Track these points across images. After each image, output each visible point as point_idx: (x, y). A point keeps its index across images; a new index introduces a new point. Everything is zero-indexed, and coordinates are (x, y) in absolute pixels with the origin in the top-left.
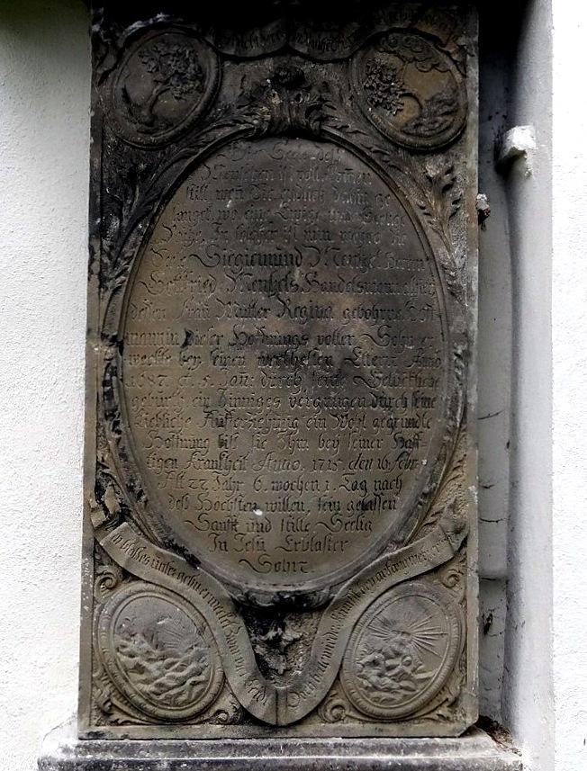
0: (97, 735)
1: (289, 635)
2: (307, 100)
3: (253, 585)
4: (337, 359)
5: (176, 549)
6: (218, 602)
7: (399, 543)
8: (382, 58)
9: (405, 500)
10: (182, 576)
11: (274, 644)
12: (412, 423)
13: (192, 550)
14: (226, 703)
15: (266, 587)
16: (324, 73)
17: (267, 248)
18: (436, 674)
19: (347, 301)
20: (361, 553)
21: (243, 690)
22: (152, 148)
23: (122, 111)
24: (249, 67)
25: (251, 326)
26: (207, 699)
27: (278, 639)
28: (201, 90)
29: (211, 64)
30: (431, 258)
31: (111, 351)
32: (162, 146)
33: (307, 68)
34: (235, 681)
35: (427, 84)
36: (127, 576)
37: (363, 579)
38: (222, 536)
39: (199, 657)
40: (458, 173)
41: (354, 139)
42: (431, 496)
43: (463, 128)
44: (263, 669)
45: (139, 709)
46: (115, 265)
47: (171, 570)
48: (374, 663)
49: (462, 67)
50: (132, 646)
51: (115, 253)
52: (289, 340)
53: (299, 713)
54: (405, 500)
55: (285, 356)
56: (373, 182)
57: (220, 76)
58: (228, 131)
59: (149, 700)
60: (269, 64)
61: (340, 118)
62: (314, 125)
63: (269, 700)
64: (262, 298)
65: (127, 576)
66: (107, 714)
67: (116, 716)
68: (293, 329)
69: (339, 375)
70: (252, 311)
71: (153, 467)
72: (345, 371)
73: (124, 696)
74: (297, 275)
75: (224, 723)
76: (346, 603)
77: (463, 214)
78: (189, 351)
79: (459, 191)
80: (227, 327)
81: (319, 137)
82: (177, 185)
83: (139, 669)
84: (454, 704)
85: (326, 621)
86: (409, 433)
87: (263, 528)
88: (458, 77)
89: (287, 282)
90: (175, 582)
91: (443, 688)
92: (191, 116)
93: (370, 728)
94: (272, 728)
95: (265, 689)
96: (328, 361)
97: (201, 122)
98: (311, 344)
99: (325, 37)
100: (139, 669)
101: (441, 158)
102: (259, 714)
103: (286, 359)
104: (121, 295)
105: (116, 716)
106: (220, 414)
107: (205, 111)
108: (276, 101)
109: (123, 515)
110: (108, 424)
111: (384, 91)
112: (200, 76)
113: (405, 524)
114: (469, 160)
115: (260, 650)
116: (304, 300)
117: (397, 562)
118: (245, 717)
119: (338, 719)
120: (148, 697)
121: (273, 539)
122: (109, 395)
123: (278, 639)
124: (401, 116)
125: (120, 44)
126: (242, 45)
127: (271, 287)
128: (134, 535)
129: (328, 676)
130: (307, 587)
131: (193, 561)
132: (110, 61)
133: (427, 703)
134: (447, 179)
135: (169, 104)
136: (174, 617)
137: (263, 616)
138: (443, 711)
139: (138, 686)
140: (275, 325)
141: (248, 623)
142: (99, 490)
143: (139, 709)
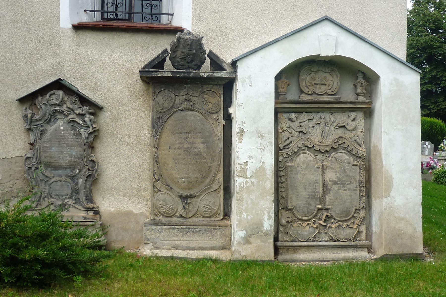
0: (155, 219)
1: (189, 202)
2: (191, 104)
3: (182, 192)
4: (197, 151)
5: (168, 186)
6: (176, 195)
7: (209, 185)
8: (205, 96)
9: (210, 177)
10: (169, 191)
11: (186, 203)
12: (211, 163)
13: (171, 186)
14: (178, 214)
15: (185, 193)
16: (195, 98)
17: (184, 131)
18: (216, 209)
19: (199, 141)
20: (202, 187)
21: (180, 211)
22: (163, 112)
23: (157, 106)
24: (181, 97)
25: (182, 145)
26: (174, 213)
27: (187, 202)
28: (172, 102)
29: (174, 97)
30: (214, 133)
31: (156, 150)
32: (165, 112)
33: (191, 97)
34: (179, 210)
35: (213, 100)
36: (159, 190)
37: (202, 192)
38: (177, 183)
39: (172, 205)
40: (219, 117)
41: (200, 111)
42: (214, 177)
43: (220, 109)
44: (184, 208)
45: (162, 215)
46: (156, 134)
47: (167, 189)
48: (204, 207)
49: (220, 97)
50: (161, 203)
51: (156, 132)
52: (188, 148)
53: (191, 216)
54: (210, 177)
55: (187, 151)
56: (203, 119)
57: (175, 99)
58: (177, 109)
59: (164, 213)
60: (184, 97)
61: (197, 106)
62: (193, 108)
63: (185, 213)
64: (183, 140)
65: (159, 190)
66: (156, 215)
67: (158, 216)
68: (189, 146)
69: (198, 154)
70: (182, 142)
71: (164, 171)
72: (198, 154)
73: (160, 212)
74: (190, 136)
75: (177, 217)
76: (199, 196)
77: (220, 125)
78: (170, 150)
79: (219, 121)
80: (177, 145)
81: (193, 111)
82: (167, 119)
83: (162, 207)
84: (219, 215)
85: (195, 199)
86: (210, 165)
87: (184, 182)
88: (219, 99)
89: (188, 137)
90: (168, 192)
91: (217, 211)
92: (170, 107)
93: (204, 219)
94: (186, 218)
95: (184, 211)
96: (195, 152)
97: (172, 108)
98: (192, 149)
99: (195, 92)
100: (162, 207)
101: (216, 114)
102: (183, 215)
103: (187, 151)
104: (157, 140)
105: (158, 216)
106: (176, 161)
107: (172, 106)
108: (186, 104)
109: (158, 180)
110: (156, 163)
111: (206, 101)
112: (172, 99)
113: (210, 182)
114: (221, 115)
115: (184, 204)
116: (191, 140)
117: (208, 189)
118: (181, 216)
119: (198, 217)
120: (164, 212)
121: (186, 184)
122: (155, 158)
123: (187, 202)
124: (208, 107)
125: (157, 93)
126: (179, 93)
127: (185, 138)
128: (161, 183)
129: (196, 209)
130: (192, 193)
131: (171, 188)
132: (155, 96)
133: (214, 214)
134: (217, 118)
135: (166, 105)
136: (168, 198)
137: (183, 198)
138: (217, 216)
139: (162, 210)
140: (186, 145)
141: (181, 200)
142: (154, 175)
143: (162, 215)
